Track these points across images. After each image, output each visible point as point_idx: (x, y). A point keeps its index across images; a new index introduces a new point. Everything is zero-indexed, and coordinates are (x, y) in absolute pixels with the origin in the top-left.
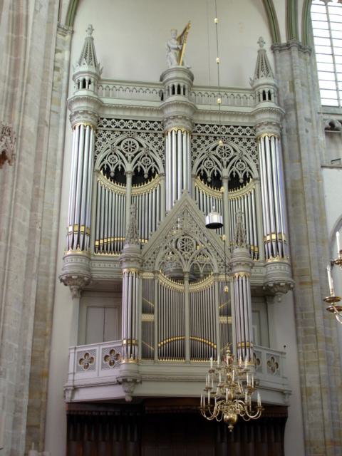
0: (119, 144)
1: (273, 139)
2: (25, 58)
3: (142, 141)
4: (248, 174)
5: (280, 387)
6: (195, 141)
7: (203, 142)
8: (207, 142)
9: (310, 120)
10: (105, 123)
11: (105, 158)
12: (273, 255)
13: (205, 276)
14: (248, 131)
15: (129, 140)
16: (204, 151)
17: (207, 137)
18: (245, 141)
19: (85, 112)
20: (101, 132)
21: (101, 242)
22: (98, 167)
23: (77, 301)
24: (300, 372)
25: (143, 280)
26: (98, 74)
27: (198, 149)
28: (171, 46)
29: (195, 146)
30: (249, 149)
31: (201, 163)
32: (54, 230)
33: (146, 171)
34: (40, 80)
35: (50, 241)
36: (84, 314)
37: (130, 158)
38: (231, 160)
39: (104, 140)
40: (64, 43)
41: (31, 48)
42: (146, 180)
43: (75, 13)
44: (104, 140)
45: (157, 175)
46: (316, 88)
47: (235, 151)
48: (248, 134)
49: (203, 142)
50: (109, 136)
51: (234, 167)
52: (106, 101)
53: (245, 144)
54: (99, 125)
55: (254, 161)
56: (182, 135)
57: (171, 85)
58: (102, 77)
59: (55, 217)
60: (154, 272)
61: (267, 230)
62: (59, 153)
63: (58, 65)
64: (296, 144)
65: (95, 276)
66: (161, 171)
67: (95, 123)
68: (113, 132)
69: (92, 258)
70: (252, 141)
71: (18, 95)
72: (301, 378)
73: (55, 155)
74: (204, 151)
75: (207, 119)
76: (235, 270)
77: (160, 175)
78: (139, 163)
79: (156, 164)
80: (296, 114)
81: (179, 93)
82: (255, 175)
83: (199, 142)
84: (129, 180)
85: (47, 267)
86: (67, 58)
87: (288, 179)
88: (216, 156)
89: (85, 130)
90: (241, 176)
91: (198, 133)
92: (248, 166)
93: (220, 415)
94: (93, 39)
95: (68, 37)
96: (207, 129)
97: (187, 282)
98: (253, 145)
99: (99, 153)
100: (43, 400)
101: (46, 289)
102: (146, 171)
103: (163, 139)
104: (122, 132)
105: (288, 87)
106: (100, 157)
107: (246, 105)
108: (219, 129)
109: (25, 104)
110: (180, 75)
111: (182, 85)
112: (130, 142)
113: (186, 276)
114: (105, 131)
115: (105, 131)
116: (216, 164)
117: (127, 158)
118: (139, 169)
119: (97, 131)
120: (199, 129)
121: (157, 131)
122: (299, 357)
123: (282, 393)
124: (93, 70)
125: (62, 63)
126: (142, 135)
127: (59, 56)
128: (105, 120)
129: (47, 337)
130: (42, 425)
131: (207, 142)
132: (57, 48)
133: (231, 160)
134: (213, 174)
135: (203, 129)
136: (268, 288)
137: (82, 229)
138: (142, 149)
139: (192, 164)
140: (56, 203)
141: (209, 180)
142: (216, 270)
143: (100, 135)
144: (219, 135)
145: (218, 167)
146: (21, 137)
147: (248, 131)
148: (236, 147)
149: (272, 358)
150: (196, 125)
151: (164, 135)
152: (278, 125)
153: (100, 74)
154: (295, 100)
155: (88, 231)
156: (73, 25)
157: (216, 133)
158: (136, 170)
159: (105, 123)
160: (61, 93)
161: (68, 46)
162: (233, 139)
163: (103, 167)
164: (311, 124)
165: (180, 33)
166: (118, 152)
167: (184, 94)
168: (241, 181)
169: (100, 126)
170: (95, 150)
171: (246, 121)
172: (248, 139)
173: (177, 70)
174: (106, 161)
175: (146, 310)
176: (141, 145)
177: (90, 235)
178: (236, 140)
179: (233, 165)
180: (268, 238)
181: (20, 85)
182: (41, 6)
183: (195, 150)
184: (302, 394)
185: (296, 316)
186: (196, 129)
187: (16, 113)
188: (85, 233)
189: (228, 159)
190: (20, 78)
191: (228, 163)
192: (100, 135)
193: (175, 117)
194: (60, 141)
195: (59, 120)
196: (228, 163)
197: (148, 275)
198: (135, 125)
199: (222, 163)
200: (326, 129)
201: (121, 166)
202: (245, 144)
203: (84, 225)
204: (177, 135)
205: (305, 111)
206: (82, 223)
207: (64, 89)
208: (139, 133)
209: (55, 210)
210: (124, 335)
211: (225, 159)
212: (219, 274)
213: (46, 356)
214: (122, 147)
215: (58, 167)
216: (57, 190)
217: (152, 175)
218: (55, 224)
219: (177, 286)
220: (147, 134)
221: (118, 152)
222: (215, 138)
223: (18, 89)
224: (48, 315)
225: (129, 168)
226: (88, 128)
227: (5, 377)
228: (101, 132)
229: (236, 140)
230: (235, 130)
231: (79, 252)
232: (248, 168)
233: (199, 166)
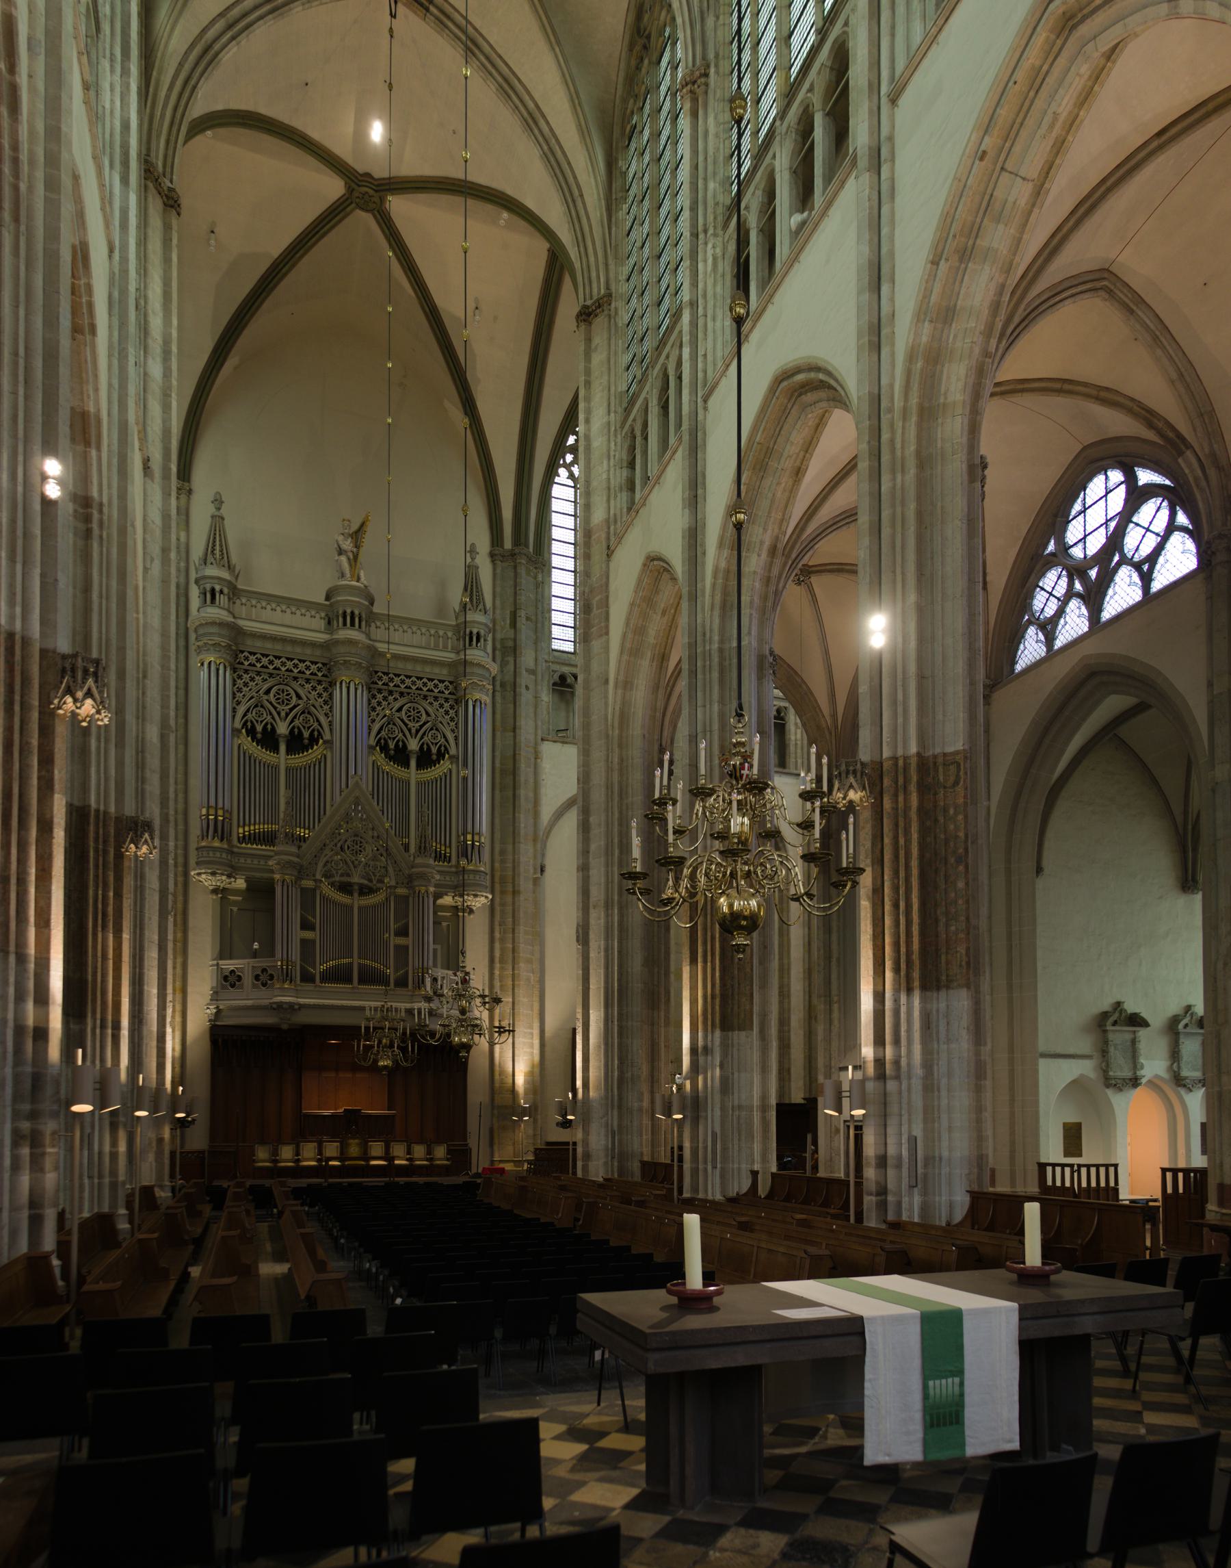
0: (268, 692)
1: (478, 703)
4: (443, 748)
6: (374, 697)
9: (532, 672)
11: (248, 711)
14: (447, 688)
15: (281, 687)
27: (379, 708)
38: (421, 727)
39: (246, 685)
42: (305, 748)
44: (246, 685)
45: (321, 741)
46: (546, 623)
47: (428, 714)
48: (447, 692)
50: (252, 679)
51: (426, 738)
53: (441, 706)
55: (453, 731)
56: (356, 689)
64: (512, 706)
66: (327, 736)
67: (232, 661)
68: (259, 673)
78: (297, 722)
80: (515, 661)
83: (380, 697)
87: (498, 754)
88: (402, 721)
89: (218, 670)
90: (434, 750)
92: (445, 737)
98: (452, 707)
99: (239, 703)
103: (330, 690)
105: (508, 622)
106: (241, 710)
112: (288, 695)
115: (246, 671)
116: (402, 731)
118: (296, 730)
119: (234, 670)
128: (246, 654)
133: (421, 727)
138: (300, 702)
139: (370, 729)
143: (240, 677)
144: (409, 691)
145: (404, 735)
146: (143, 752)
147: (447, 688)
148: (430, 709)
154: (515, 640)
157: (403, 686)
158: (292, 731)
159: (247, 659)
162: (425, 697)
163: (245, 724)
164: (533, 677)
168: (434, 757)
169: (239, 663)
170: (234, 698)
171: (443, 673)
174: (249, 716)
178: (430, 700)
179: (424, 734)
183: (374, 709)
191: (417, 731)
192: (240, 677)
196: (417, 731)
199: (410, 730)
200: (554, 684)
201: (272, 724)
202: (441, 706)
204: (348, 688)
205: (527, 658)
208: (295, 679)
226: (221, 668)
229: (430, 700)
230: (429, 683)
232: (443, 740)
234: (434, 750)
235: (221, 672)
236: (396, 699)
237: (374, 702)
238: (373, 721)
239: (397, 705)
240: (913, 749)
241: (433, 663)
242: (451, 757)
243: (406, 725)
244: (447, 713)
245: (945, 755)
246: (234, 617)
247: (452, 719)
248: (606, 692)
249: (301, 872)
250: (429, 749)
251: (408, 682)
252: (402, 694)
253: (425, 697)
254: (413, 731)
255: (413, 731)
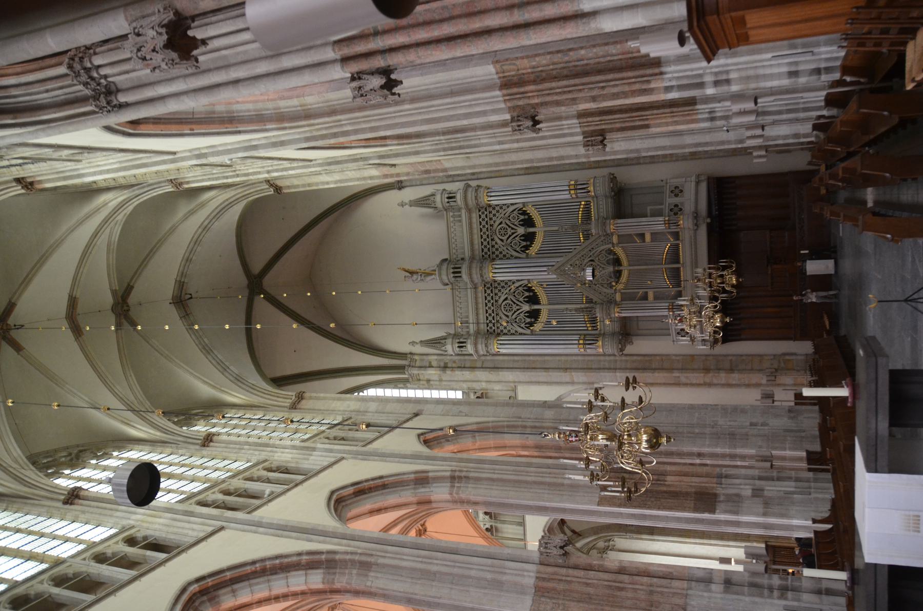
1: (489, 194)
2: (504, 421)
3: (503, 298)
5: (693, 184)
6: (497, 256)
7: (497, 250)
8: (496, 246)
10: (491, 328)
12: (589, 192)
13: (615, 254)
16: (505, 248)
17: (493, 246)
18: (491, 215)
19: (486, 346)
20: (499, 331)
21: (588, 325)
22: (528, 332)
23: (634, 338)
24: (677, 160)
25: (622, 300)
26: (451, 336)
27: (504, 253)
28: (419, 279)
29: (501, 256)
30: (498, 211)
31: (515, 251)
32: (580, 358)
33: (527, 294)
34: (514, 408)
35: (589, 361)
36: (644, 332)
37: (518, 307)
38: (509, 227)
40: (422, 360)
41: (494, 417)
42: (535, 294)
43: (395, 353)
49: (497, 250)
52: (472, 328)
53: (494, 215)
54: (493, 333)
55: (508, 207)
57: (453, 279)
58: (452, 332)
59: (569, 358)
60: (616, 293)
61: (568, 196)
62: (516, 358)
63: (442, 364)
65: (617, 330)
66: (526, 282)
69: (602, 332)
70: (491, 209)
71: (532, 424)
72: (683, 160)
73: (518, 361)
74: (505, 248)
75: (477, 246)
76: (609, 232)
77: (529, 283)
78: (521, 299)
79: (520, 286)
81: (460, 272)
82: (521, 206)
83: (497, 253)
84: (536, 307)
85: (610, 361)
86: (436, 357)
88: (508, 238)
90: (522, 217)
91: (489, 255)
93: (733, 286)
94: (421, 341)
95: (416, 357)
96: (485, 247)
97: (621, 268)
98: (494, 209)
99: (516, 331)
100: (711, 358)
101: (627, 361)
102: (527, 294)
104: (497, 315)
107: (460, 216)
108: (485, 237)
109: (536, 419)
110: (444, 272)
111: (452, 270)
113: (616, 268)
114: (498, 328)
117: (518, 310)
119: (499, 335)
120: (486, 253)
121: (492, 287)
122: (667, 162)
123: (698, 183)
124: (449, 341)
125: (440, 360)
126: (497, 298)
127: (434, 364)
129: (664, 358)
130: (730, 358)
131: (496, 246)
132: (428, 365)
133: (509, 227)
134: (523, 240)
135: (486, 250)
136: (615, 195)
137: (581, 342)
139: (516, 258)
140: (558, 358)
141: (528, 243)
142: (610, 246)
143: (502, 331)
148: (497, 223)
149: (672, 192)
150: (483, 256)
151: (495, 281)
152: (476, 191)
153: (450, 334)
155: (582, 337)
156: (406, 354)
160: (465, 360)
161: (425, 357)
162: (491, 225)
163: (527, 327)
165: (408, 274)
166: (514, 316)
167: (460, 268)
168: (526, 217)
171: (475, 216)
172: (490, 212)
173: (440, 275)
174: (523, 325)
175: (645, 297)
176: (506, 299)
177: (585, 335)
180: (574, 196)
181: (524, 423)
182: (460, 412)
183: (504, 256)
184: (696, 159)
185: (633, 164)
186: (487, 256)
187: (544, 425)
188: (584, 340)
189: (509, 229)
190: (520, 423)
191: (513, 229)
192: (502, 331)
193: (481, 276)
194: (506, 358)
195: (488, 360)
196: (513, 229)
197: (618, 297)
198: (489, 305)
199: (513, 234)
203: (579, 340)
206: (577, 342)
207: (462, 358)
208: (496, 301)
209: (563, 358)
210: (666, 313)
211: (510, 231)
212: (613, 244)
213: (678, 358)
214: (510, 314)
215: (527, 358)
216: (547, 358)
217: (529, 289)
218: (574, 358)
219: (625, 274)
220: (496, 294)
221: (514, 316)
222: (492, 240)
223: (529, 424)
224: (647, 358)
225: (526, 307)
226: (499, 342)
227: (717, 421)
228: (499, 331)
229: (492, 222)
231: (600, 343)
233: (518, 252)
234: (522, 217)
235: (501, 342)
236: (496, 243)
237: (501, 256)
238: (512, 256)
239: (499, 242)
240: (498, 93)
241: (470, 224)
242: (524, 207)
243: (510, 236)
244: (498, 211)
245: (497, 73)
246: (470, 335)
247: (501, 208)
248: (474, 157)
249: (611, 302)
250: (522, 220)
251: (485, 237)
252: (492, 240)
253: (491, 225)
254: (513, 231)
255: (513, 231)
